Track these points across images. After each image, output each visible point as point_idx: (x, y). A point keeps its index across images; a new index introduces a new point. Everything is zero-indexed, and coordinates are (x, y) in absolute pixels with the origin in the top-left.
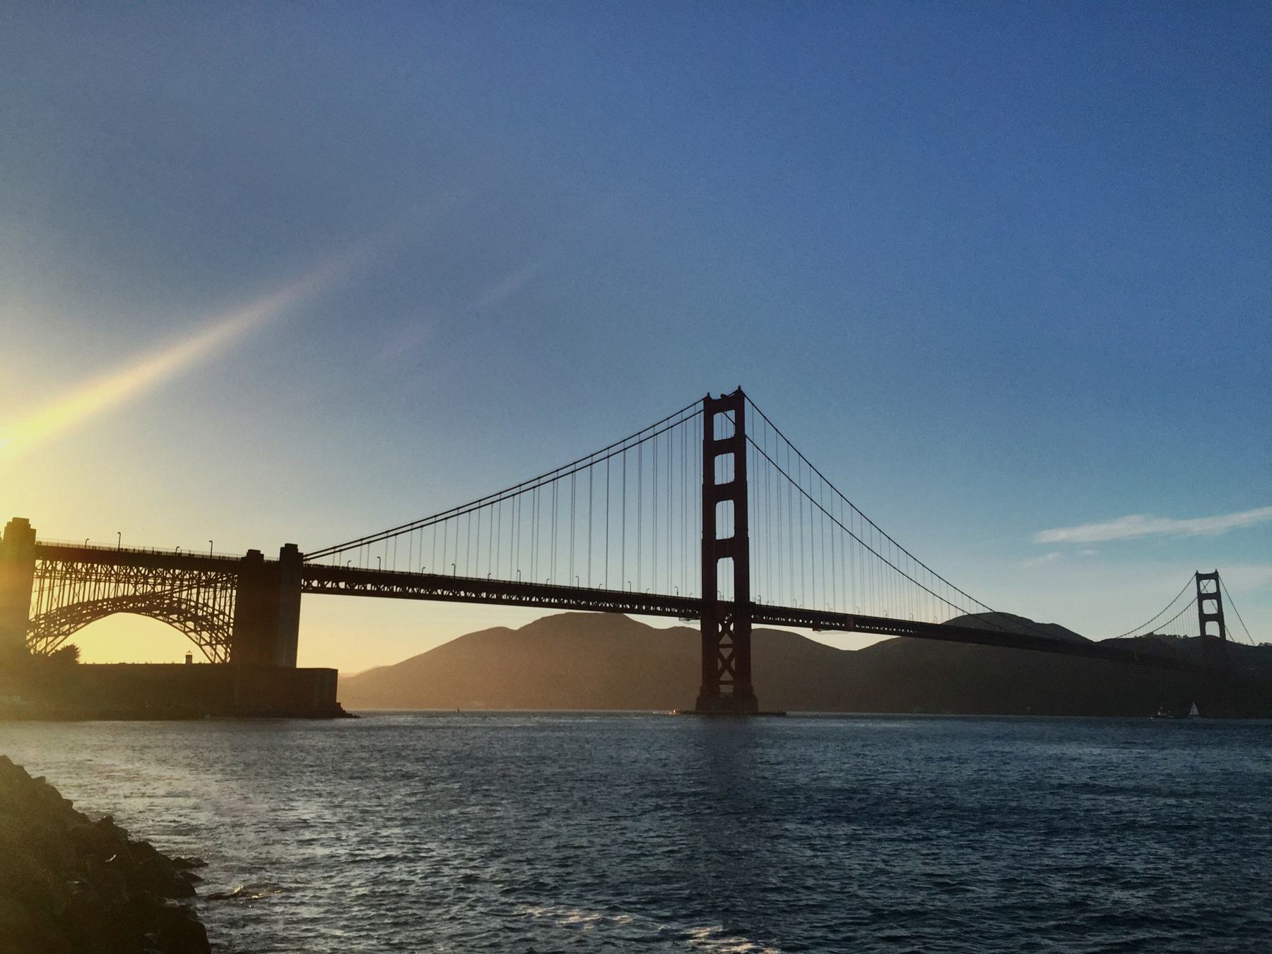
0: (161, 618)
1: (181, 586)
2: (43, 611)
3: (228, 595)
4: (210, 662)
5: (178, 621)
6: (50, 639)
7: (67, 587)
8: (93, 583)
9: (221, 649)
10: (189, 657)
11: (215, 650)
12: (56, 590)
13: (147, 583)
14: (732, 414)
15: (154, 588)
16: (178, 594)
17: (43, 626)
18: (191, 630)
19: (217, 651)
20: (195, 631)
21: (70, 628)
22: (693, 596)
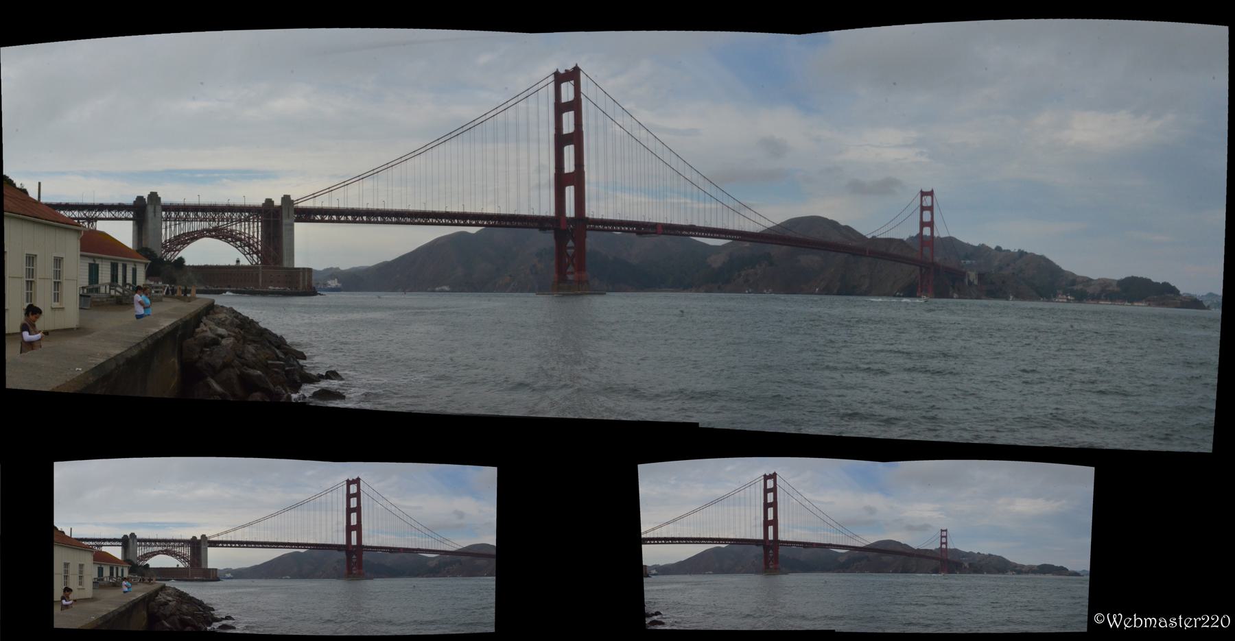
1: (232, 222)
2: (168, 238)
3: (255, 226)
4: (250, 264)
6: (172, 253)
9: (255, 256)
10: (238, 261)
12: (173, 227)
13: (215, 221)
14: (572, 82)
15: (218, 224)
18: (239, 247)
20: (241, 246)
22: (548, 214)
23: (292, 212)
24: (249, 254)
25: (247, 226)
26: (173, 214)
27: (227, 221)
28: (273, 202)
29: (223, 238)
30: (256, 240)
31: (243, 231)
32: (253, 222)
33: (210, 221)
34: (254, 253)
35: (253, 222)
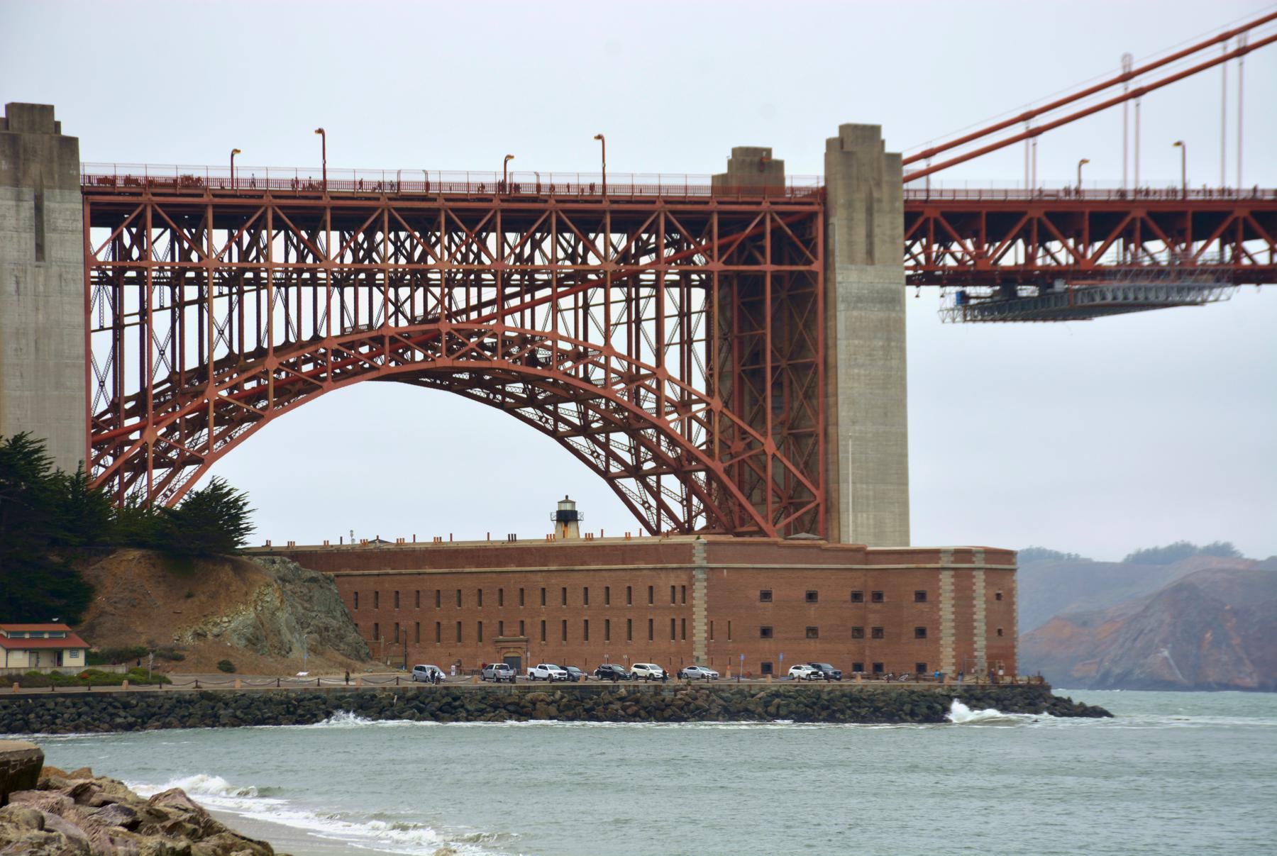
0: (478, 391)
2: (132, 386)
5: (531, 401)
6: (159, 474)
7: (191, 313)
8: (322, 291)
9: (671, 483)
10: (567, 517)
11: (656, 494)
12: (161, 323)
13: (426, 284)
16: (517, 315)
17: (135, 436)
18: (576, 431)
19: (663, 496)
20: (584, 430)
21: (213, 439)
23: (891, 224)
24: (635, 471)
25: (617, 311)
26: (161, 243)
27: (503, 281)
28: (779, 165)
29: (477, 381)
30: (671, 392)
31: (596, 338)
32: (658, 286)
33: (396, 283)
34: (664, 466)
35: (658, 286)
